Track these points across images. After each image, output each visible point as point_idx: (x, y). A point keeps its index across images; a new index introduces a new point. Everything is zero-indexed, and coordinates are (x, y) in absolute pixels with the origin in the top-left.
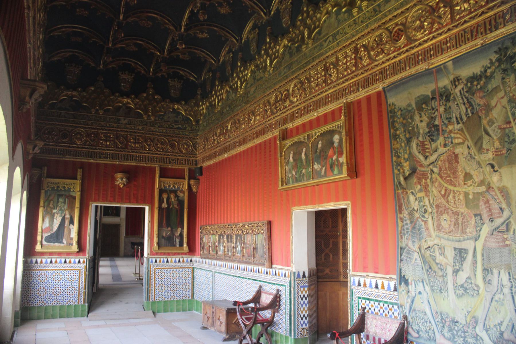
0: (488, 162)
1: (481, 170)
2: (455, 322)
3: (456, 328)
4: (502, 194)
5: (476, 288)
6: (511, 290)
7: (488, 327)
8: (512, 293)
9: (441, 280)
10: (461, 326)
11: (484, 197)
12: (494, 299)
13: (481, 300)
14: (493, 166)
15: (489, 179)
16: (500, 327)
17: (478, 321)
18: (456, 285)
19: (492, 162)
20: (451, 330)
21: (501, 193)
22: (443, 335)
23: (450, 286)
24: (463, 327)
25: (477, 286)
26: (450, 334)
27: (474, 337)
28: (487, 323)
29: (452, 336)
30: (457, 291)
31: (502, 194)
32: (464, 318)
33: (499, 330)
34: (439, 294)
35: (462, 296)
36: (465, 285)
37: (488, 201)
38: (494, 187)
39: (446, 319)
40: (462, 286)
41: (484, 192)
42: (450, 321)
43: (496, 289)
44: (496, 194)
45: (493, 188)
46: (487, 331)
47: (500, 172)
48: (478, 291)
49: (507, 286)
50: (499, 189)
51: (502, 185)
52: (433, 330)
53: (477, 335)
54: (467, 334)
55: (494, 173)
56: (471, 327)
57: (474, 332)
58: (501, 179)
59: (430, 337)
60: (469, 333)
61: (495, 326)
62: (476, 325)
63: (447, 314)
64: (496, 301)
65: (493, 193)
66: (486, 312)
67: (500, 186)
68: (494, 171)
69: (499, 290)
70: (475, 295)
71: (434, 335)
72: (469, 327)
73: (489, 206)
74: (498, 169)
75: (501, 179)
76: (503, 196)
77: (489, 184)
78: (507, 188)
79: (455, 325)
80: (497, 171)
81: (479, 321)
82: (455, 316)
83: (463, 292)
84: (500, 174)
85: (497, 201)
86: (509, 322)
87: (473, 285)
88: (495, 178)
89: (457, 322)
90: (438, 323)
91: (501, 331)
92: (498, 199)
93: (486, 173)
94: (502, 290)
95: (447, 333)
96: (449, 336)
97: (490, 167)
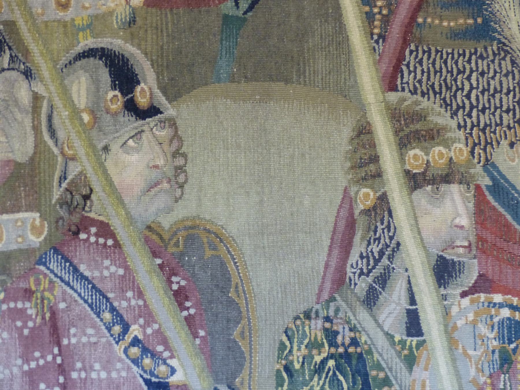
0: (86, 42)
1: (23, 93)
4: (178, 281)
11: (28, 294)
14: (124, 76)
15: (84, 165)
19: (118, 44)
21: (168, 271)
31: (178, 281)
37: (54, 329)
38: (117, 224)
41: (27, 252)
44: (128, 281)
45: (105, 230)
47: (172, 123)
50: (155, 240)
51: (183, 211)
55: (133, 124)
58: (177, 176)
65: (105, 271)
67: (166, 222)
68: (131, 107)
73: (62, 369)
74: (161, 100)
75: (177, 176)
76: (180, 297)
77: (79, 196)
78: (218, 237)
80: (153, 111)
84: (176, 136)
85: (135, 331)
88: (130, 166)
92: (147, 315)
93: (62, 114)
97: (105, 76)
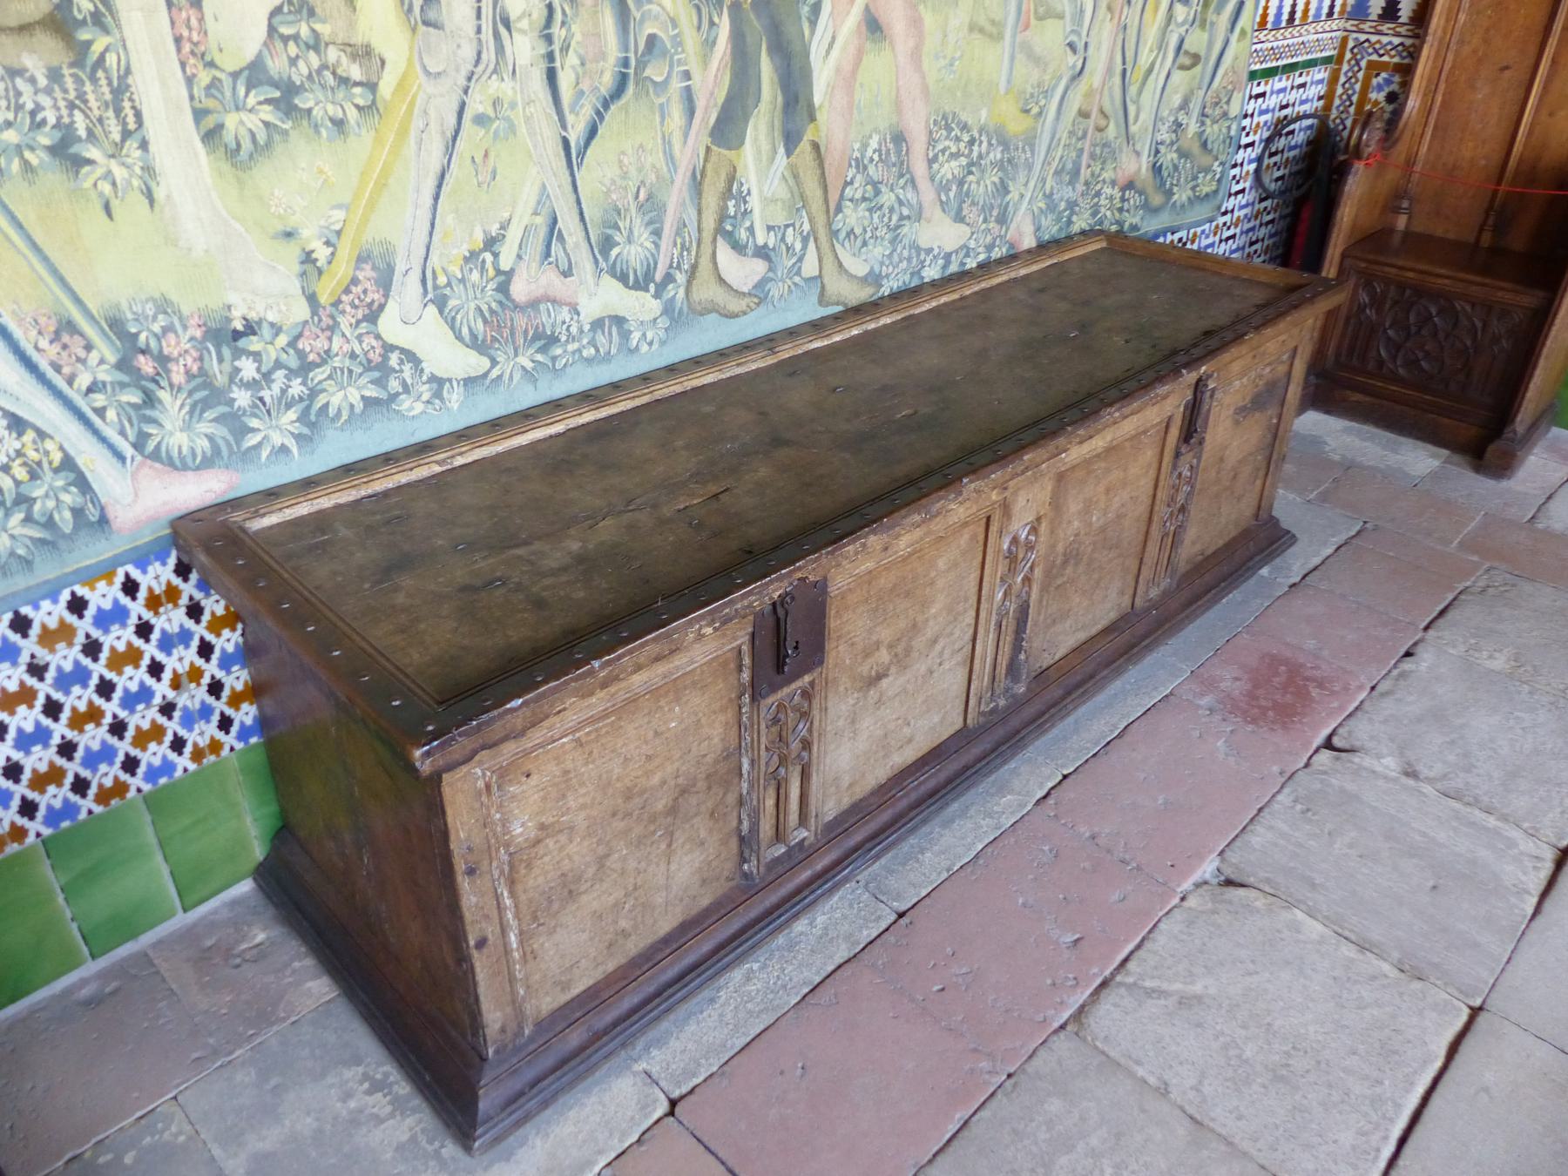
2: (237, 335)
3: (248, 369)
5: (356, 73)
6: (549, 39)
7: (442, 280)
8: (550, 57)
9: (34, 64)
10: (282, 340)
12: (468, 115)
13: (402, 133)
16: (496, 255)
17: (390, 269)
18: (204, 77)
20: (206, 395)
22: (155, 456)
23: (159, 91)
24: (292, 343)
25: (363, 53)
26: (204, 427)
27: (369, 367)
28: (434, 260)
29: (221, 432)
30: (231, 121)
32: (295, 286)
33: (491, 273)
34: (53, 178)
35: (269, 144)
36: (277, 65)
39: (170, 347)
40: (255, 73)
42: (200, 345)
43: (468, 52)
46: (441, 302)
48: (372, 87)
49: (524, 24)
52: (68, 464)
53: (389, 348)
54: (319, 374)
56: (345, 322)
57: (370, 341)
59: (50, 524)
60: (337, 362)
61: (472, 257)
62: (386, 296)
63: (163, 306)
64: (480, 120)
66: (429, 201)
69: (489, 55)
70: (352, 114)
71: (82, 483)
72: (333, 328)
79: (238, 353)
81: (400, 267)
82: (232, 298)
83: (267, 113)
86: (535, 213)
87: (332, 54)
89: (251, 329)
90: (99, 399)
91: (499, 272)
94: (500, 50)
95: (187, 427)
96: (203, 444)
